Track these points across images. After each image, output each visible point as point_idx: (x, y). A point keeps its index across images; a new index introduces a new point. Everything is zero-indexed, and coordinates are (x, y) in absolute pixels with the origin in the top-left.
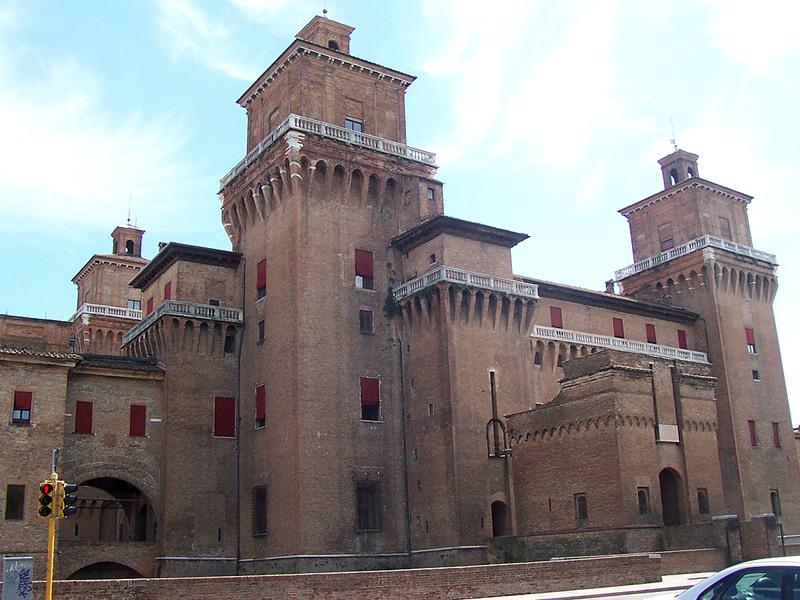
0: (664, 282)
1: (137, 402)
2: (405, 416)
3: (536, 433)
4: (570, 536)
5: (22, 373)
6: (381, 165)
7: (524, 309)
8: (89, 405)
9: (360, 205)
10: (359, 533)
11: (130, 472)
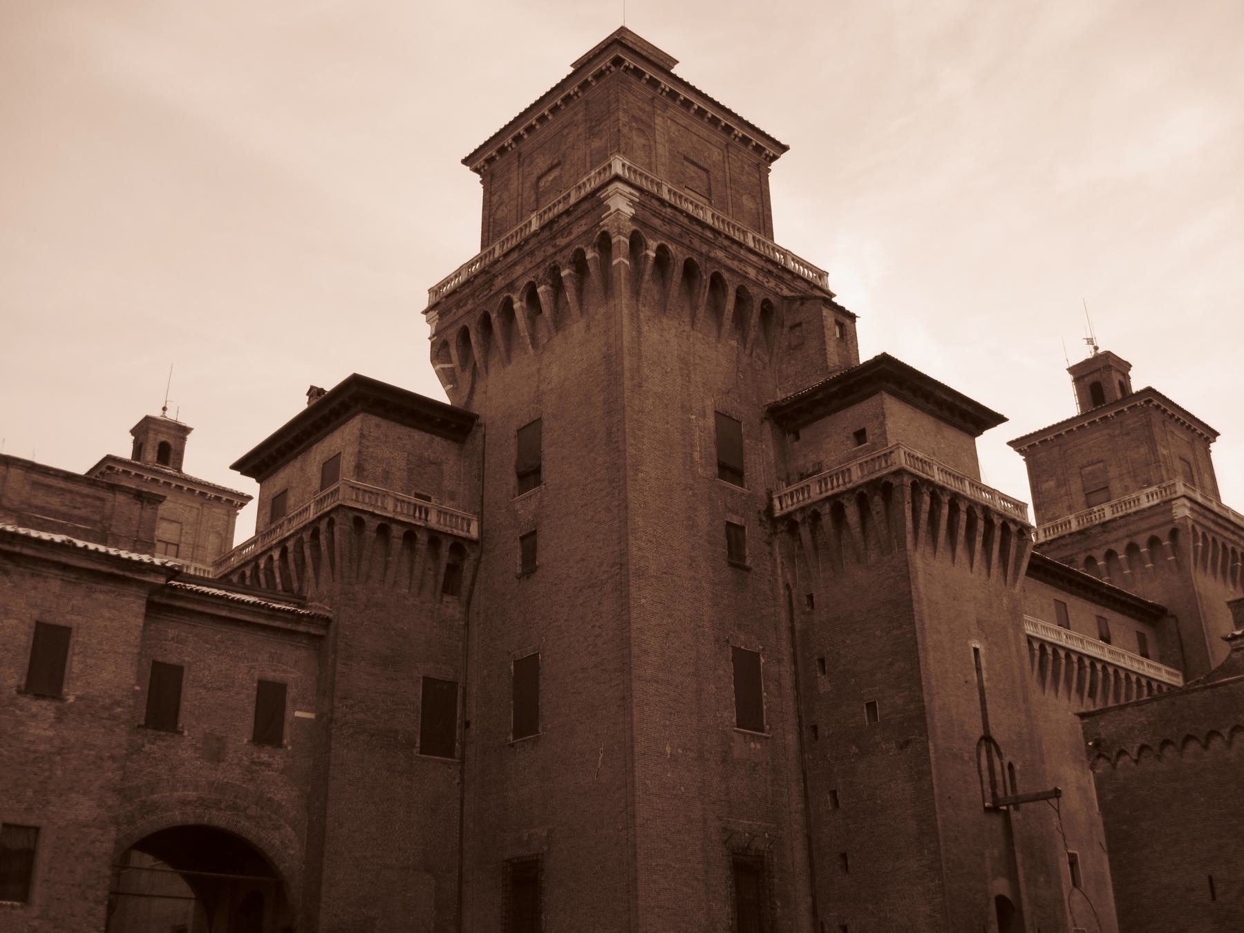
0: (1099, 555)
1: (271, 675)
2: (810, 732)
3: (1166, 743)
5: (55, 585)
6: (752, 273)
7: (1014, 541)
8: (177, 671)
9: (719, 336)
11: (249, 818)
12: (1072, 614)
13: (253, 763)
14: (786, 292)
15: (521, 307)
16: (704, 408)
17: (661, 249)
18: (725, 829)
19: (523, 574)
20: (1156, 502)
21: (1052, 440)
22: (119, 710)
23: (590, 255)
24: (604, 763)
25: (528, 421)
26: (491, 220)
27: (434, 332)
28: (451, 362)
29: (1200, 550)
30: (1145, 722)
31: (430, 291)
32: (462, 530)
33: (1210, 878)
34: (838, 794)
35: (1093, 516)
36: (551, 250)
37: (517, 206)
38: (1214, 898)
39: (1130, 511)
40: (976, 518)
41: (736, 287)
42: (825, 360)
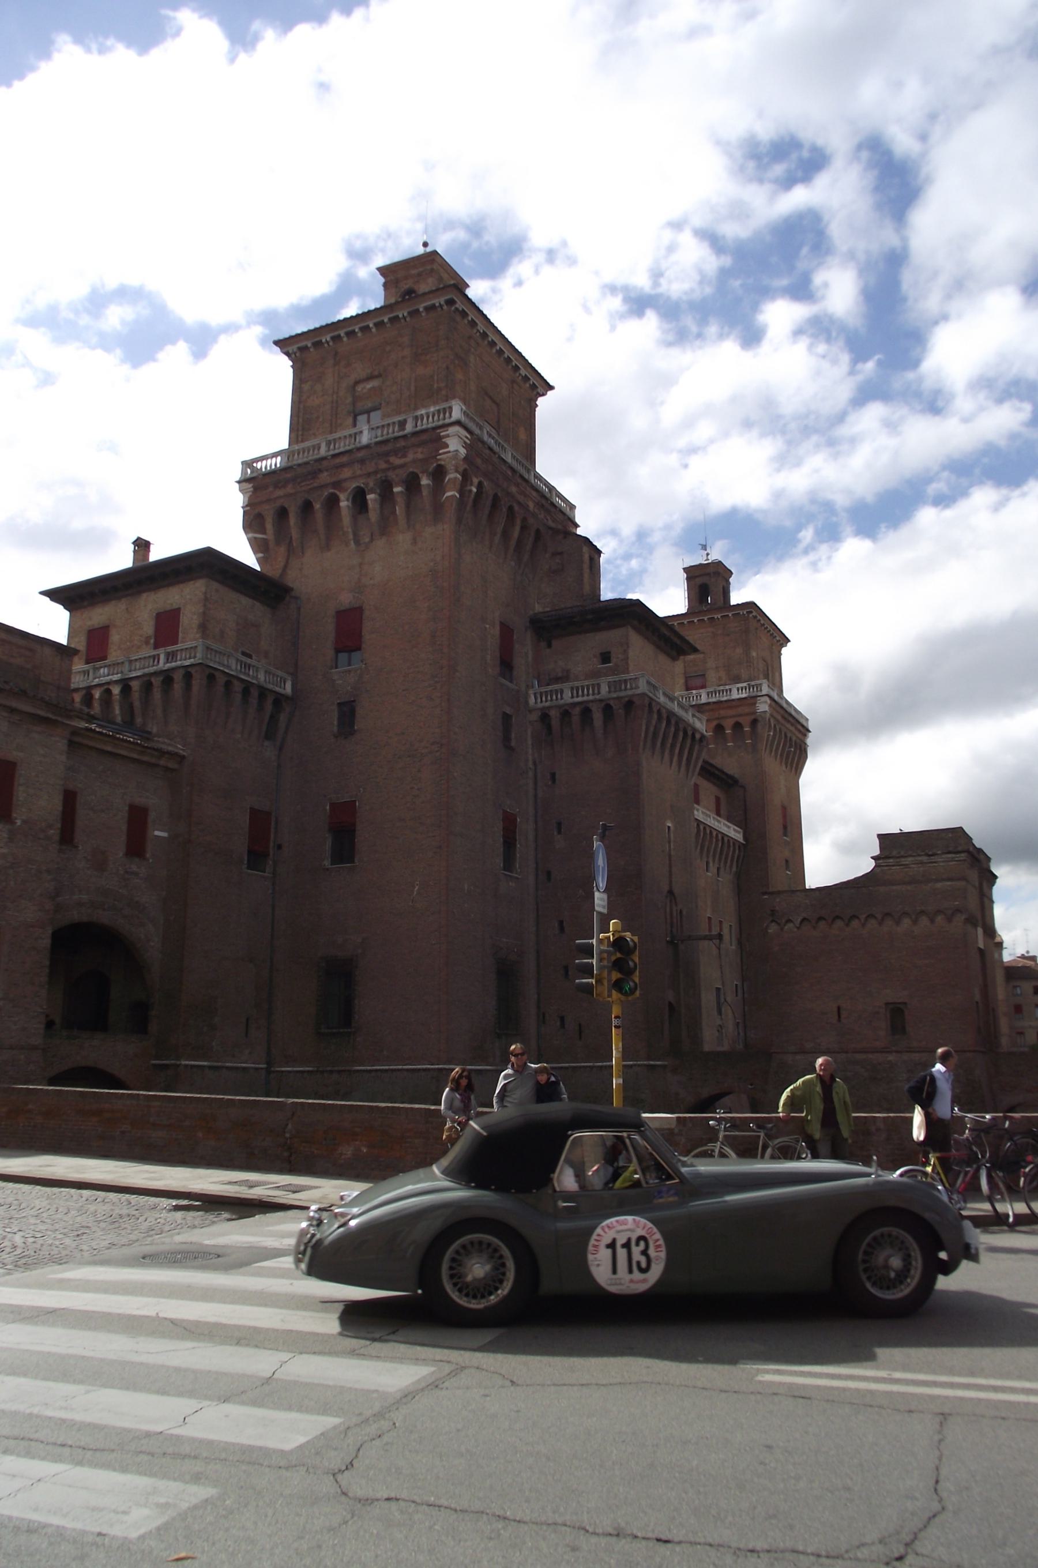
6: (531, 505)
7: (697, 747)
13: (127, 872)
14: (551, 523)
15: (348, 506)
17: (480, 484)
20: (744, 695)
22: (52, 831)
23: (425, 481)
26: (302, 406)
27: (246, 503)
28: (264, 532)
29: (770, 738)
31: (243, 463)
32: (280, 687)
33: (839, 1008)
34: (565, 923)
36: (383, 465)
37: (332, 402)
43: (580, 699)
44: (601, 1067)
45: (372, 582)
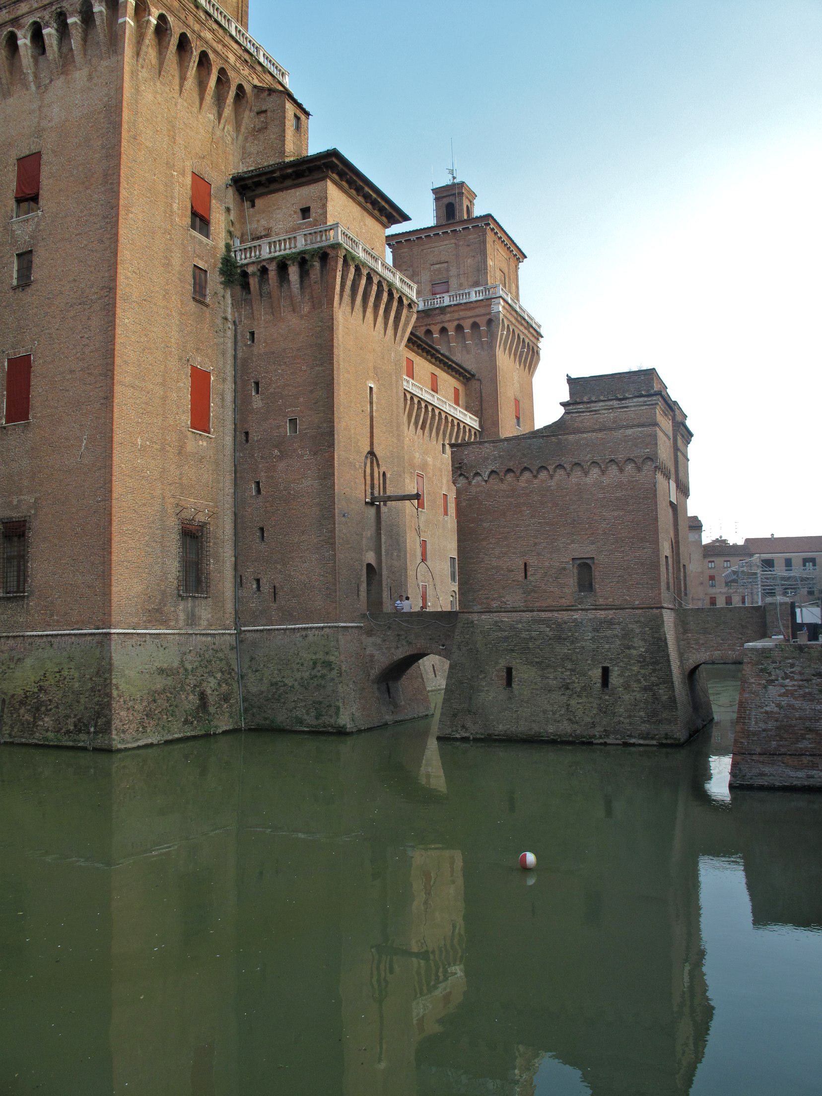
2: (243, 436)
3: (509, 470)
4: (564, 616)
6: (232, 59)
10: (183, 598)
12: (416, 369)
14: (256, 82)
16: (184, 167)
17: (162, 18)
18: (178, 505)
19: (18, 287)
20: (481, 298)
21: (414, 240)
24: (86, 448)
25: (28, 153)
30: (497, 455)
33: (525, 564)
35: (436, 300)
38: (526, 577)
39: (462, 302)
40: (383, 290)
41: (218, 68)
42: (284, 145)
43: (277, 254)
44: (294, 629)
45: (50, 125)
